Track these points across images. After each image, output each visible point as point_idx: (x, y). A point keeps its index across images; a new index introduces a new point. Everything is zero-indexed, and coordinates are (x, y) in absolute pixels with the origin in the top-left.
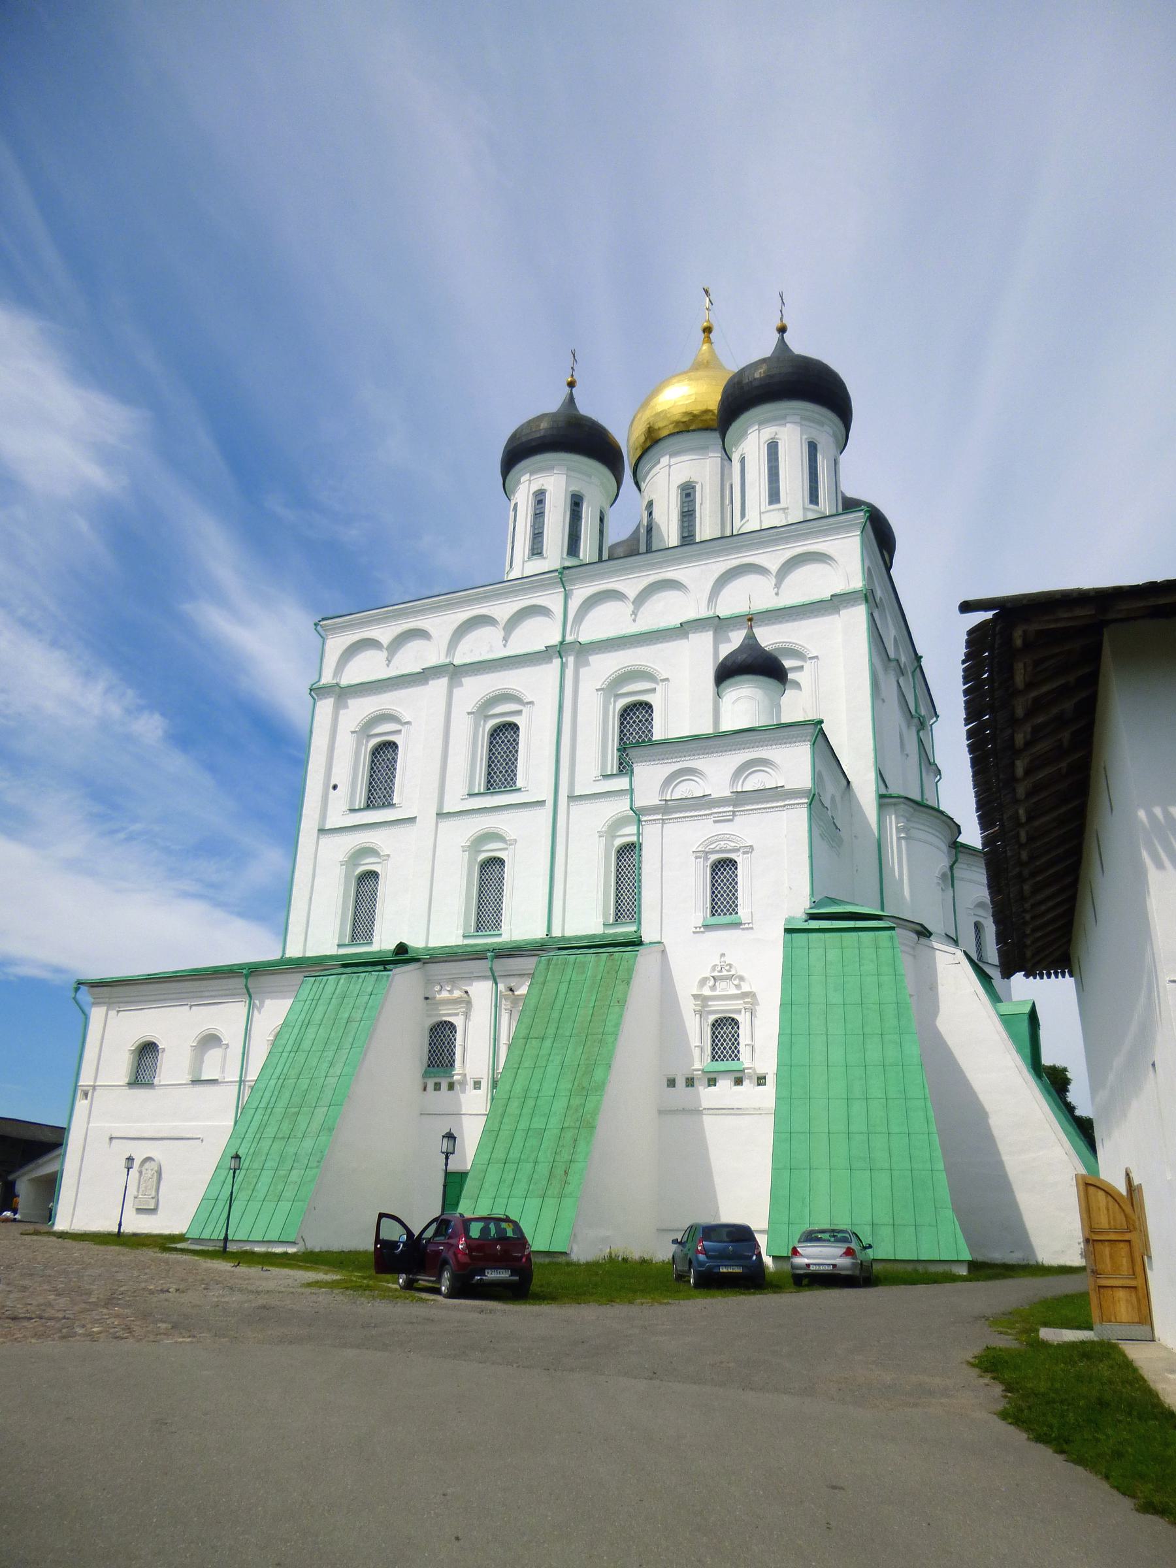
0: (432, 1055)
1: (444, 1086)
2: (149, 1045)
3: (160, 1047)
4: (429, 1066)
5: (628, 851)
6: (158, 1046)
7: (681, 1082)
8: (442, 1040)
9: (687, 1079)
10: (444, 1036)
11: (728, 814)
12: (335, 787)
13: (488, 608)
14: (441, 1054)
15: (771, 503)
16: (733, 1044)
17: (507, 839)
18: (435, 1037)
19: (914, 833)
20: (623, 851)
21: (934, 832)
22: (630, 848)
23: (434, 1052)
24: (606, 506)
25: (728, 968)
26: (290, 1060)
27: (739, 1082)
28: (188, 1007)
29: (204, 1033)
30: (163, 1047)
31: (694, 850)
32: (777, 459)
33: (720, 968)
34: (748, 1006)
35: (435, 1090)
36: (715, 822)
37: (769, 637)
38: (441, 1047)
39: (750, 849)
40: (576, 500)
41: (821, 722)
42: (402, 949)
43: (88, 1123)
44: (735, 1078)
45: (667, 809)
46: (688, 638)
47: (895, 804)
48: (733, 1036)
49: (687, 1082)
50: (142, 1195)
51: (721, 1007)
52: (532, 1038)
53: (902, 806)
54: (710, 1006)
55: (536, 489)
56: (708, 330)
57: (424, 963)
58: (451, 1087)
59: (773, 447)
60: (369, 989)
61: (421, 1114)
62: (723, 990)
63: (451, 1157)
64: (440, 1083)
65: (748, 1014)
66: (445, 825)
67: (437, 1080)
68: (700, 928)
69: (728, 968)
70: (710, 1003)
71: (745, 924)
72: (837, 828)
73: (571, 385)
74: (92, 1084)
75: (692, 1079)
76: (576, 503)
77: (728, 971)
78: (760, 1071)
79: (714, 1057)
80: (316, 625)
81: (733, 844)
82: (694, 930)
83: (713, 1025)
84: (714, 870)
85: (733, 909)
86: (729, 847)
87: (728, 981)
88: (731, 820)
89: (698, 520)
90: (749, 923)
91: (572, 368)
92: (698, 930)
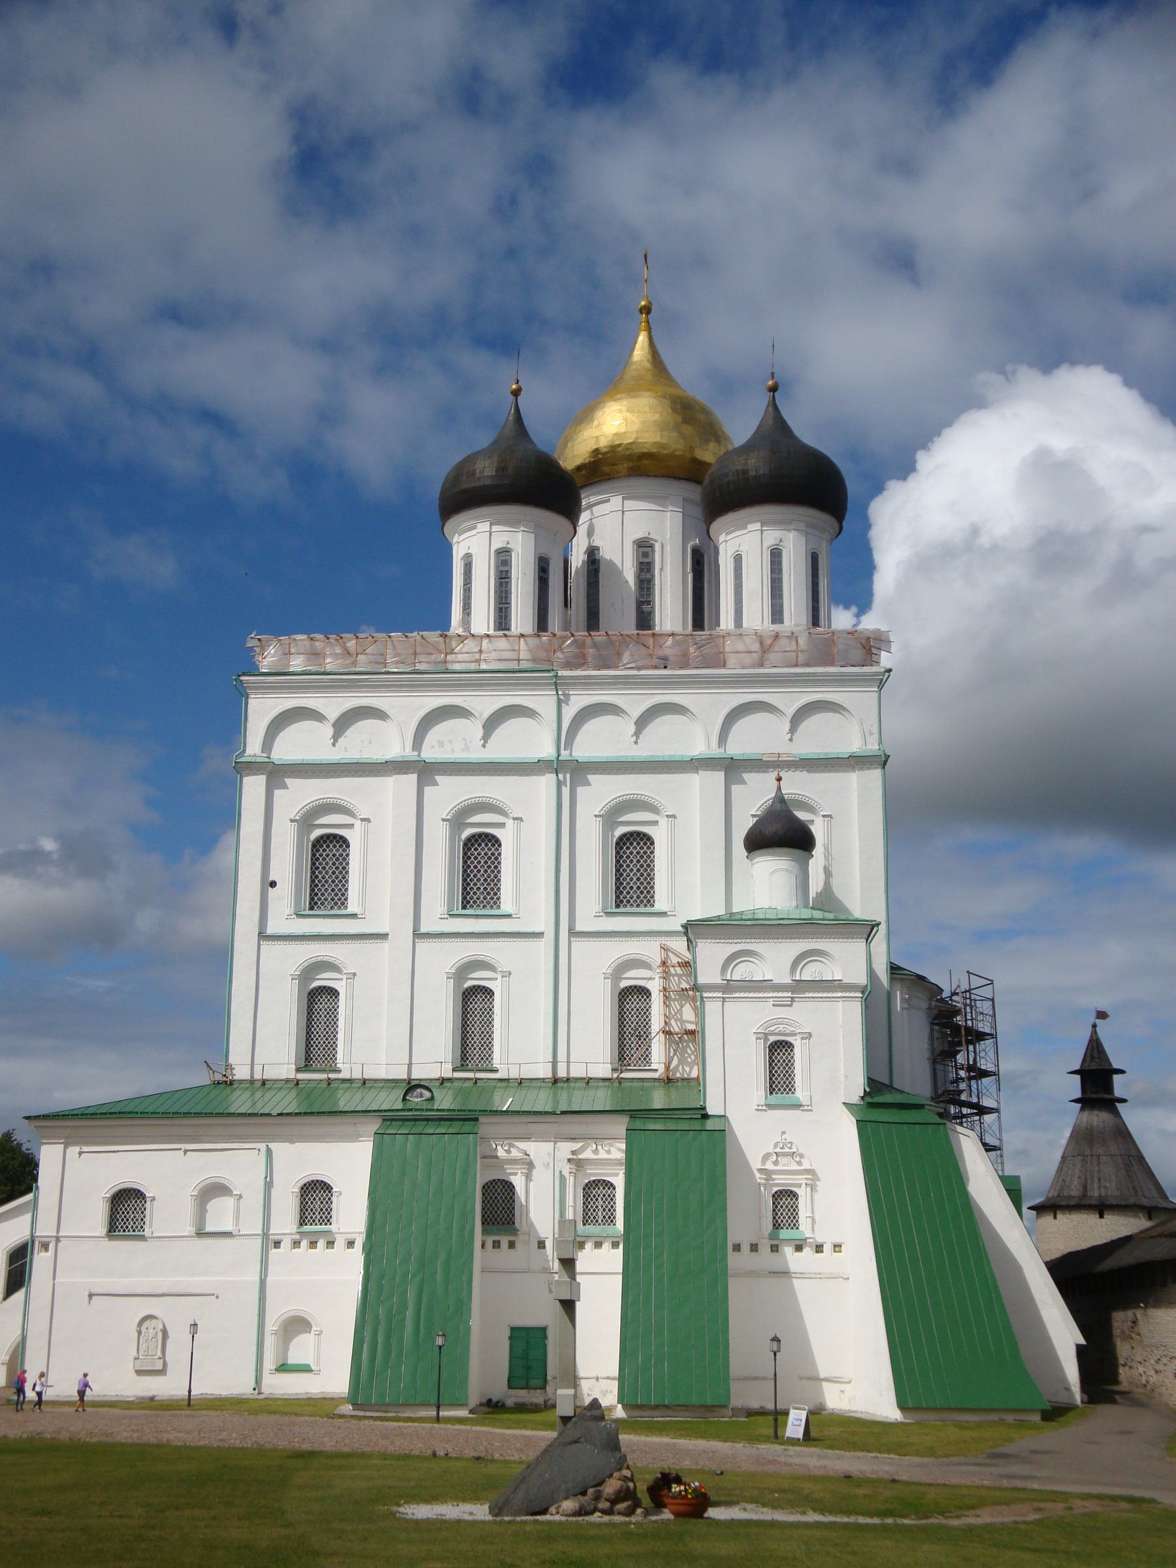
3: (147, 1196)
6: (145, 1195)
7: (746, 1248)
11: (787, 999)
12: (273, 884)
13: (461, 698)
20: (625, 994)
25: (790, 1145)
27: (799, 1248)
28: (181, 1152)
29: (207, 1182)
30: (152, 1195)
31: (755, 1031)
32: (780, 571)
33: (782, 1146)
35: (494, 1247)
36: (774, 1005)
40: (546, 566)
43: (54, 1279)
44: (796, 1245)
45: (729, 988)
46: (698, 773)
49: (751, 1248)
50: (143, 1356)
51: (781, 1181)
54: (774, 1180)
55: (500, 545)
58: (512, 1245)
59: (776, 555)
62: (784, 1165)
64: (499, 1242)
66: (423, 946)
67: (496, 1238)
68: (762, 1106)
69: (790, 1145)
70: (774, 1176)
71: (805, 1106)
73: (516, 393)
74: (55, 1234)
77: (790, 1148)
78: (820, 1240)
81: (793, 1029)
82: (757, 1107)
85: (790, 1088)
86: (787, 1031)
87: (789, 1157)
88: (791, 1006)
89: (657, 588)
90: (808, 1106)
92: (760, 1107)
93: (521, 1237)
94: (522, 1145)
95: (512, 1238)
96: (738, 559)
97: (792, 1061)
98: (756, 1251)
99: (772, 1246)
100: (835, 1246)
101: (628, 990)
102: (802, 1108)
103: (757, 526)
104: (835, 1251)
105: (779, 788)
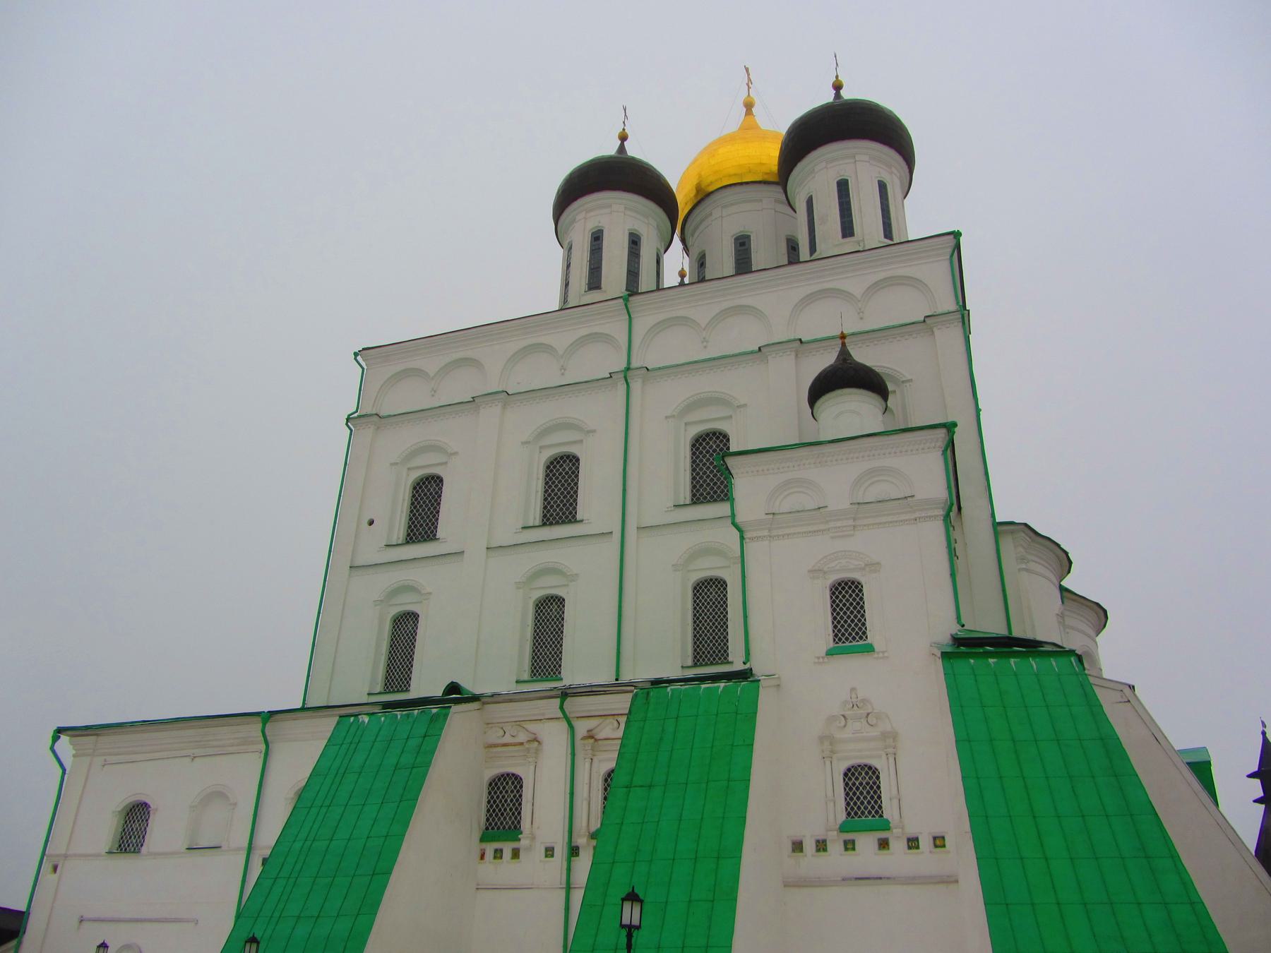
0: (491, 815)
1: (507, 853)
2: (138, 806)
4: (487, 829)
5: (706, 587)
7: (809, 846)
8: (503, 797)
9: (818, 841)
10: (507, 792)
12: (371, 523)
14: (502, 814)
15: (844, 236)
16: (872, 797)
17: (568, 574)
18: (495, 793)
19: (1032, 566)
21: (1046, 565)
22: (708, 584)
23: (494, 811)
24: (662, 251)
26: (320, 818)
27: (884, 844)
28: (188, 759)
34: (890, 750)
35: (495, 858)
36: (832, 538)
37: (863, 355)
38: (503, 805)
39: (874, 567)
41: (955, 425)
42: (453, 688)
44: (879, 840)
47: (1012, 532)
48: (872, 788)
49: (817, 846)
52: (635, 787)
53: (1023, 535)
56: (749, 106)
57: (484, 703)
58: (516, 854)
59: (843, 187)
60: (423, 731)
61: (477, 889)
63: (635, 933)
64: (501, 850)
65: (891, 760)
68: (823, 658)
72: (955, 555)
75: (824, 841)
76: (634, 242)
78: (911, 831)
79: (849, 814)
80: (356, 355)
83: (846, 775)
84: (833, 593)
87: (862, 720)
90: (883, 652)
91: (624, 123)
93: (524, 843)
94: (532, 727)
95: (515, 845)
96: (810, 202)
97: (861, 603)
98: (825, 850)
99: (846, 843)
100: (935, 838)
101: (703, 584)
102: (876, 655)
103: (823, 164)
104: (936, 846)
105: (844, 344)
